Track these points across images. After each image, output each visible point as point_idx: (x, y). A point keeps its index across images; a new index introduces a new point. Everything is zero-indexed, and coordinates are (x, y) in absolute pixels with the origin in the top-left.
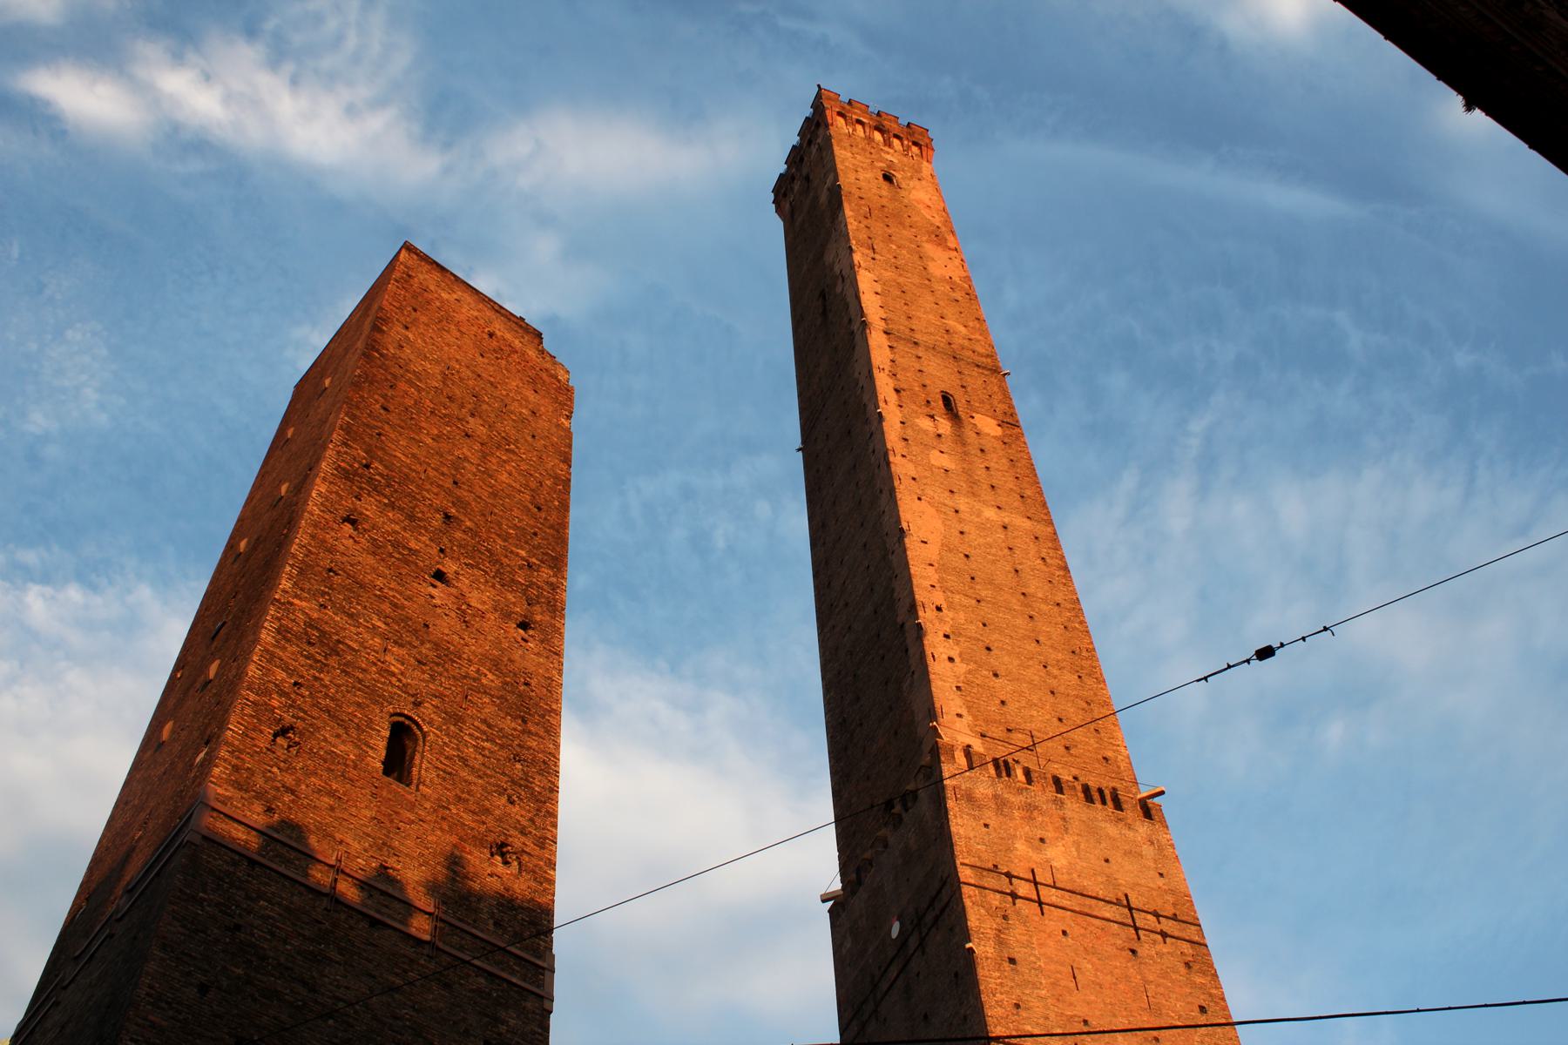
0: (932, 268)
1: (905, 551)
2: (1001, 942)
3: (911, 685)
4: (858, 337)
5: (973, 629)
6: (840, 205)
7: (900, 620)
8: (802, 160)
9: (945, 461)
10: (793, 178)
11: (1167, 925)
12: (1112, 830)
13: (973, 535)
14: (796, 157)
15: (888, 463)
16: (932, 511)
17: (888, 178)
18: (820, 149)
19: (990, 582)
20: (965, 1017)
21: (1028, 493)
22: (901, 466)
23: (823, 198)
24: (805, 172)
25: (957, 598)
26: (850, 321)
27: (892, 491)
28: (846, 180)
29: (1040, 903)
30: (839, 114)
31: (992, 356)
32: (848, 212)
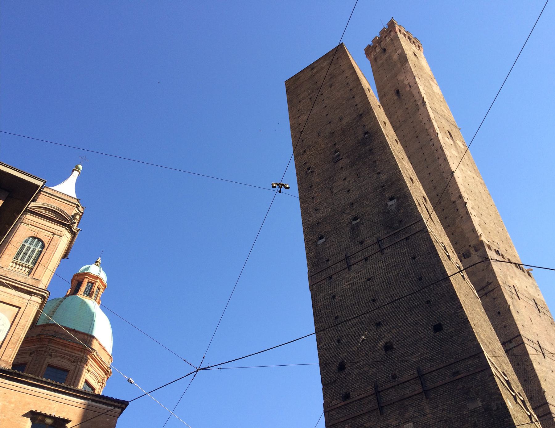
2: (514, 306)
3: (461, 221)
4: (422, 108)
5: (476, 207)
6: (406, 60)
7: (453, 199)
11: (543, 310)
12: (525, 278)
13: (467, 178)
14: (378, 42)
15: (443, 150)
17: (415, 55)
20: (505, 327)
22: (447, 152)
23: (395, 57)
25: (470, 197)
26: (415, 101)
27: (445, 159)
29: (518, 297)
32: (411, 65)
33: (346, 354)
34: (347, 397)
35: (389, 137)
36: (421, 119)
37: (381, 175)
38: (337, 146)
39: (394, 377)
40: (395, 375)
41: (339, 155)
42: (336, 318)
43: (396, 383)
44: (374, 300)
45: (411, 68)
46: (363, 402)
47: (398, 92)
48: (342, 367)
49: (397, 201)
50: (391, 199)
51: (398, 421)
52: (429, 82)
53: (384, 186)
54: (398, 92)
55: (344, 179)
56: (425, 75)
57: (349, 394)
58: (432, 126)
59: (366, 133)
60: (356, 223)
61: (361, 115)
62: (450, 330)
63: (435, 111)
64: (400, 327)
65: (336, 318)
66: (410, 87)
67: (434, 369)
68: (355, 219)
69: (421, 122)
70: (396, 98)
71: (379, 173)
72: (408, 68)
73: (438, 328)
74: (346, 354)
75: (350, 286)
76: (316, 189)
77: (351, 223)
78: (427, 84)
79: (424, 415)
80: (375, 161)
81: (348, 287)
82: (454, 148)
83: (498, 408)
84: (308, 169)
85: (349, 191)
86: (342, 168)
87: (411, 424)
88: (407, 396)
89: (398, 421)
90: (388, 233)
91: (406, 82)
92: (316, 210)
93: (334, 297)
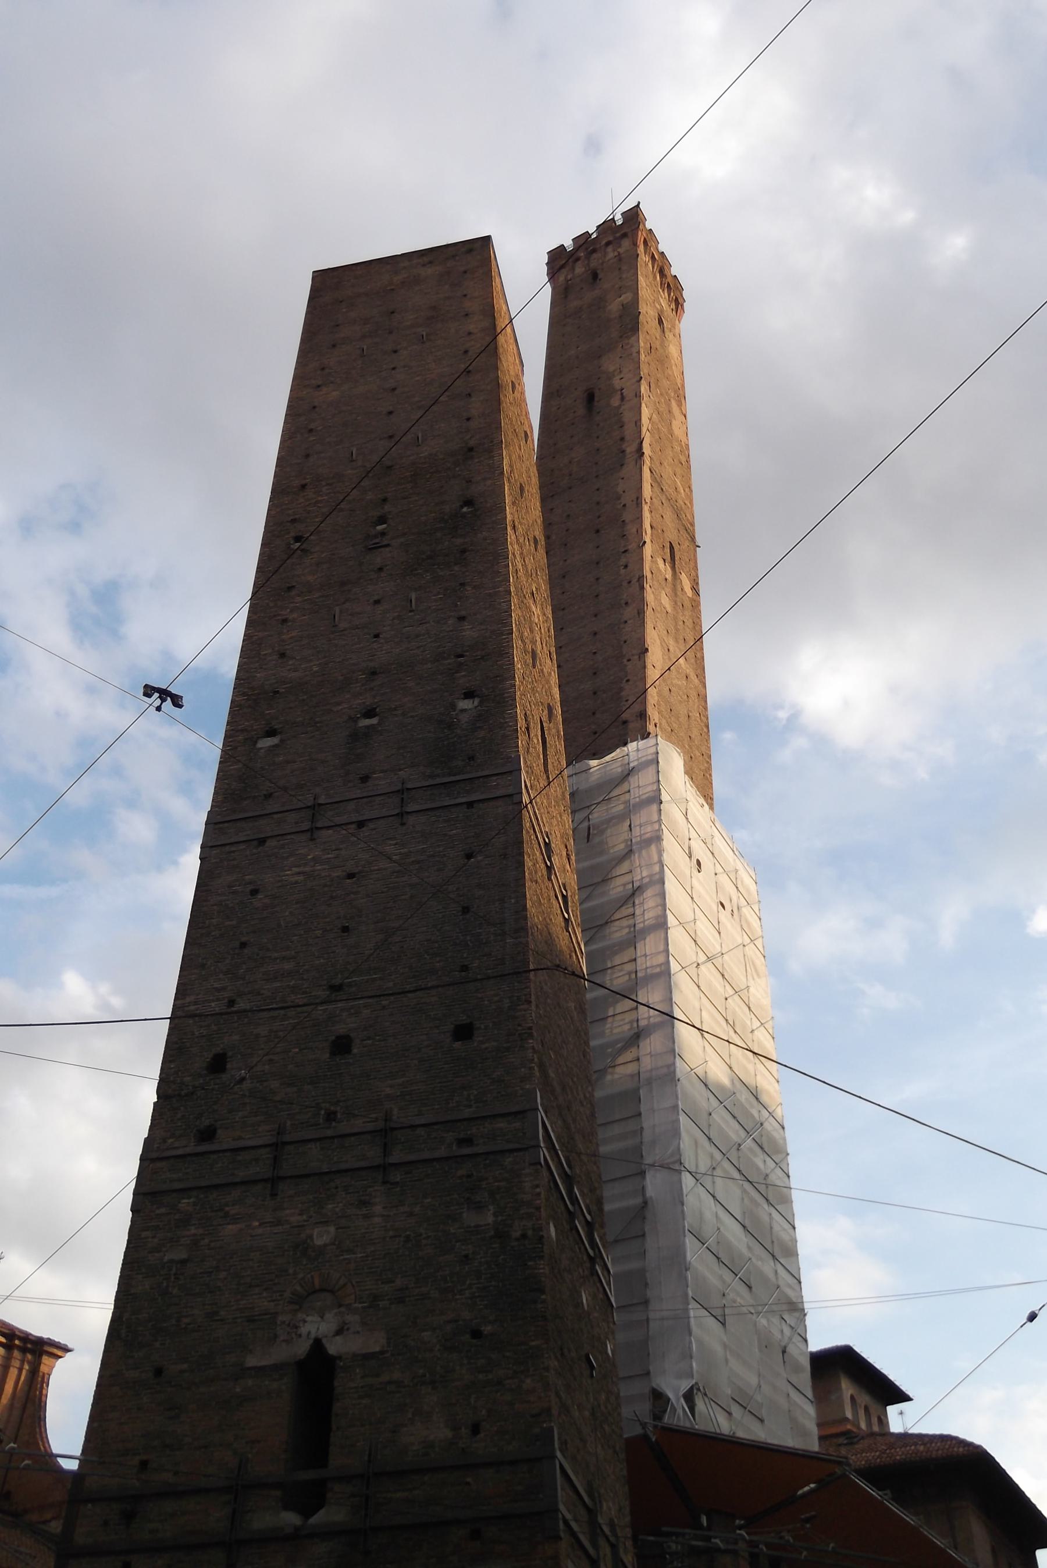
0: (674, 422)
1: (645, 667)
7: (625, 716)
8: (594, 251)
9: (666, 602)
10: (578, 259)
15: (642, 588)
16: (658, 642)
17: (660, 322)
18: (620, 258)
19: (678, 718)
21: (698, 655)
22: (649, 596)
23: (614, 307)
24: (594, 264)
26: (622, 439)
27: (641, 613)
28: (643, 308)
30: (645, 242)
31: (692, 525)
32: (642, 344)
33: (236, 1037)
34: (207, 1135)
35: (520, 529)
36: (620, 489)
37: (466, 626)
38: (387, 507)
39: (331, 1117)
40: (335, 1113)
41: (383, 534)
42: (243, 945)
43: (329, 1133)
44: (345, 929)
45: (639, 352)
46: (239, 1158)
47: (590, 398)
48: (218, 1064)
49: (481, 703)
50: (469, 695)
51: (305, 1217)
52: (669, 406)
53: (462, 656)
54: (590, 398)
55: (377, 602)
56: (665, 383)
57: (215, 1131)
58: (640, 518)
59: (468, 503)
60: (367, 727)
61: (471, 449)
62: (487, 1045)
63: (657, 482)
64: (384, 1008)
65: (243, 945)
66: (623, 398)
67: (423, 1121)
68: (370, 713)
69: (619, 498)
70: (581, 411)
71: (462, 619)
72: (634, 350)
73: (464, 1032)
74: (236, 1037)
75: (301, 878)
76: (299, 599)
77: (355, 720)
78: (663, 408)
79: (366, 1217)
80: (462, 585)
81: (297, 878)
82: (668, 590)
83: (524, 1236)
84: (298, 539)
85: (377, 636)
86: (381, 569)
87: (332, 1229)
88: (343, 1166)
89: (305, 1217)
90: (432, 776)
91: (617, 383)
92: (282, 655)
93: (254, 892)
